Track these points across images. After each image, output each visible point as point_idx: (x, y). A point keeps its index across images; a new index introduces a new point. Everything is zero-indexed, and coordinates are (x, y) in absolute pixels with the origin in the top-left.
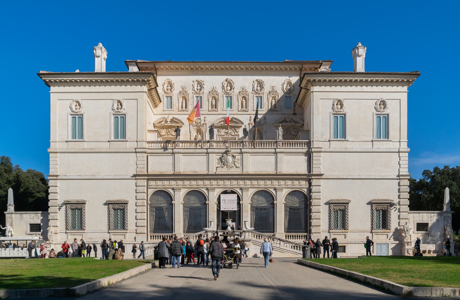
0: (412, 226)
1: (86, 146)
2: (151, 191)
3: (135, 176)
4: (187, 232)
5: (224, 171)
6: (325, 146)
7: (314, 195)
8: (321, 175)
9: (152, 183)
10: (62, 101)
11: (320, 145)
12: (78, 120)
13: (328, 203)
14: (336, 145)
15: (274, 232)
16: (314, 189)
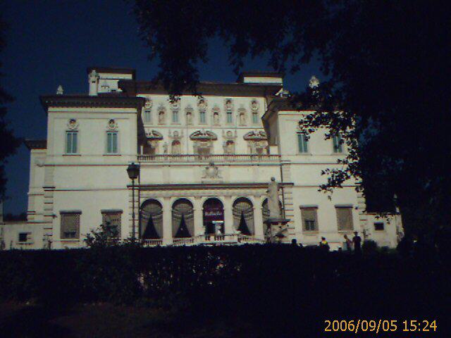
0: (371, 228)
1: (82, 160)
2: (142, 200)
3: (128, 186)
4: (176, 237)
5: (209, 180)
6: (293, 159)
7: (286, 201)
8: (293, 184)
9: (144, 193)
10: (58, 121)
11: (289, 158)
12: (72, 138)
13: (301, 208)
14: (302, 159)
15: (254, 234)
16: (286, 196)
